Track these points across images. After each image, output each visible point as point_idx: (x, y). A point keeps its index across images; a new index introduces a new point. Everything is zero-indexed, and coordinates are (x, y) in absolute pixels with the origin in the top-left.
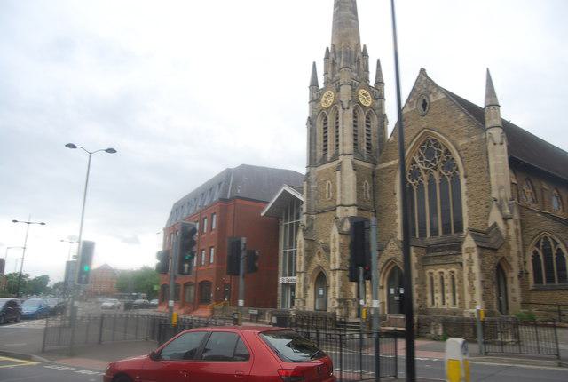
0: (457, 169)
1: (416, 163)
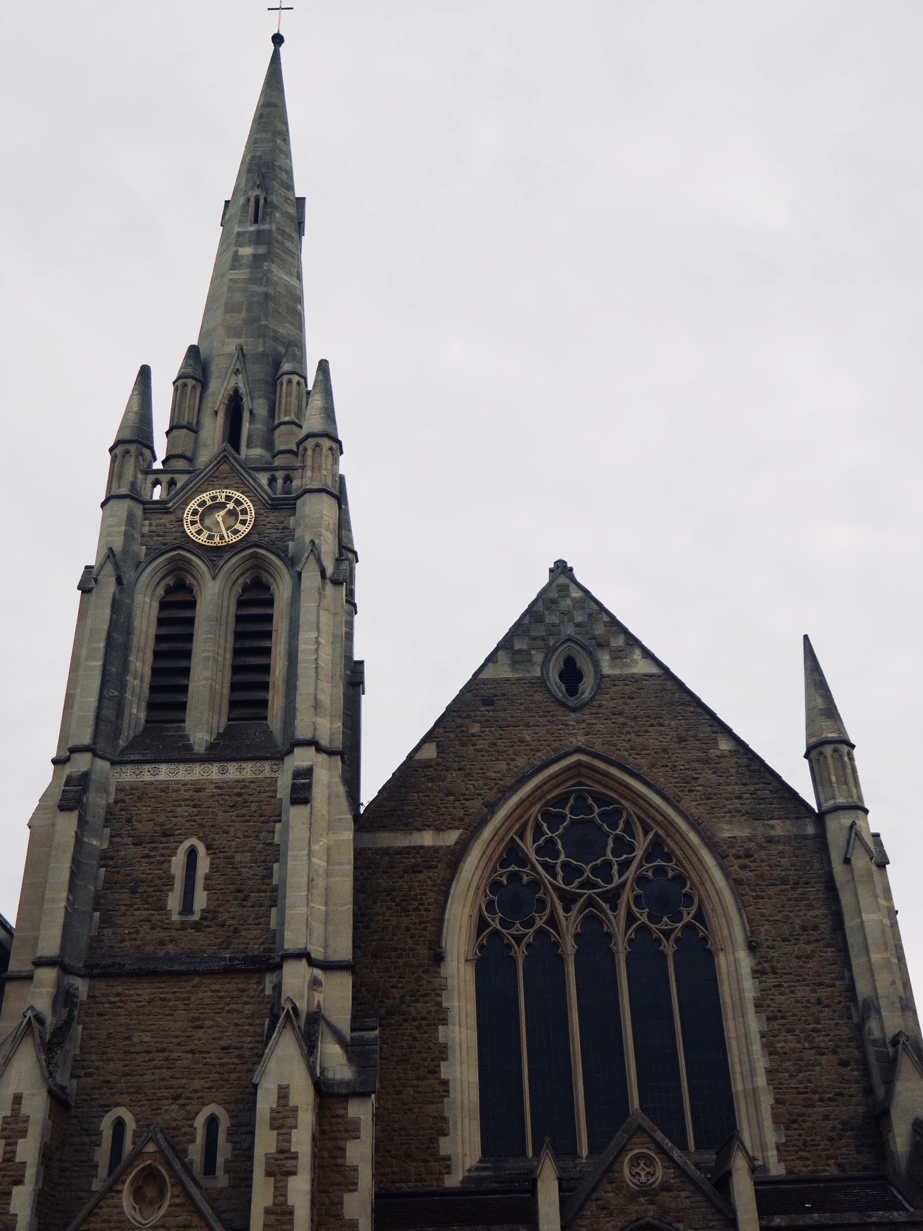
0: (700, 916)
1: (524, 861)
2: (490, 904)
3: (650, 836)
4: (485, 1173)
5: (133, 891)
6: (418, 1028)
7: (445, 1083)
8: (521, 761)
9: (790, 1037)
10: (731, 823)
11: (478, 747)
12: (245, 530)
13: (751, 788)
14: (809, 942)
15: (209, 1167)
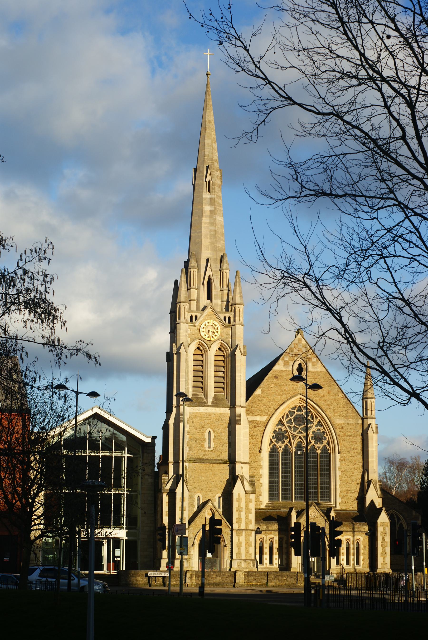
0: (328, 443)
1: (283, 425)
2: (273, 437)
3: (318, 420)
4: (270, 505)
5: (196, 441)
6: (255, 469)
7: (261, 483)
8: (284, 396)
9: (346, 477)
10: (339, 419)
11: (273, 391)
12: (218, 335)
13: (346, 409)
14: (354, 453)
15: (219, 507)
